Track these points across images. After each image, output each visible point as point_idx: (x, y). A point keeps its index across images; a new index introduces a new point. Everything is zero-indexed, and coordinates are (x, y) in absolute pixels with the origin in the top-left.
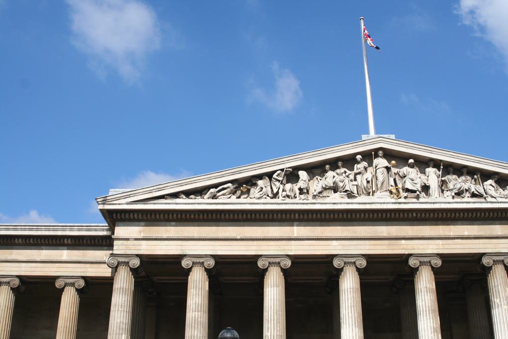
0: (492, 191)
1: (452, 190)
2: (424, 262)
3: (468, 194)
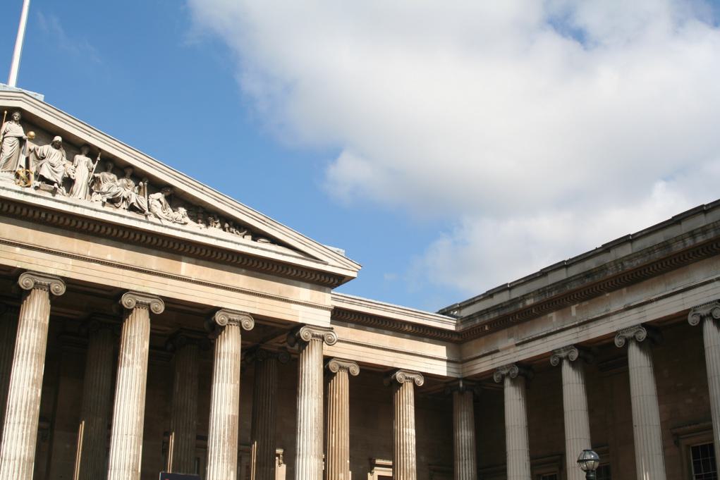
0: (157, 208)
1: (104, 193)
2: (41, 284)
3: (124, 205)
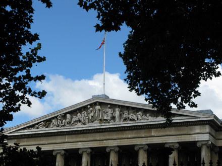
0: (140, 117)
